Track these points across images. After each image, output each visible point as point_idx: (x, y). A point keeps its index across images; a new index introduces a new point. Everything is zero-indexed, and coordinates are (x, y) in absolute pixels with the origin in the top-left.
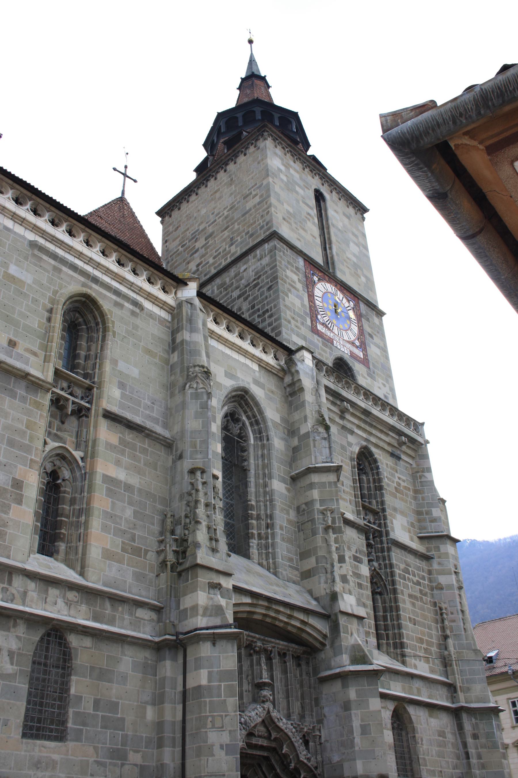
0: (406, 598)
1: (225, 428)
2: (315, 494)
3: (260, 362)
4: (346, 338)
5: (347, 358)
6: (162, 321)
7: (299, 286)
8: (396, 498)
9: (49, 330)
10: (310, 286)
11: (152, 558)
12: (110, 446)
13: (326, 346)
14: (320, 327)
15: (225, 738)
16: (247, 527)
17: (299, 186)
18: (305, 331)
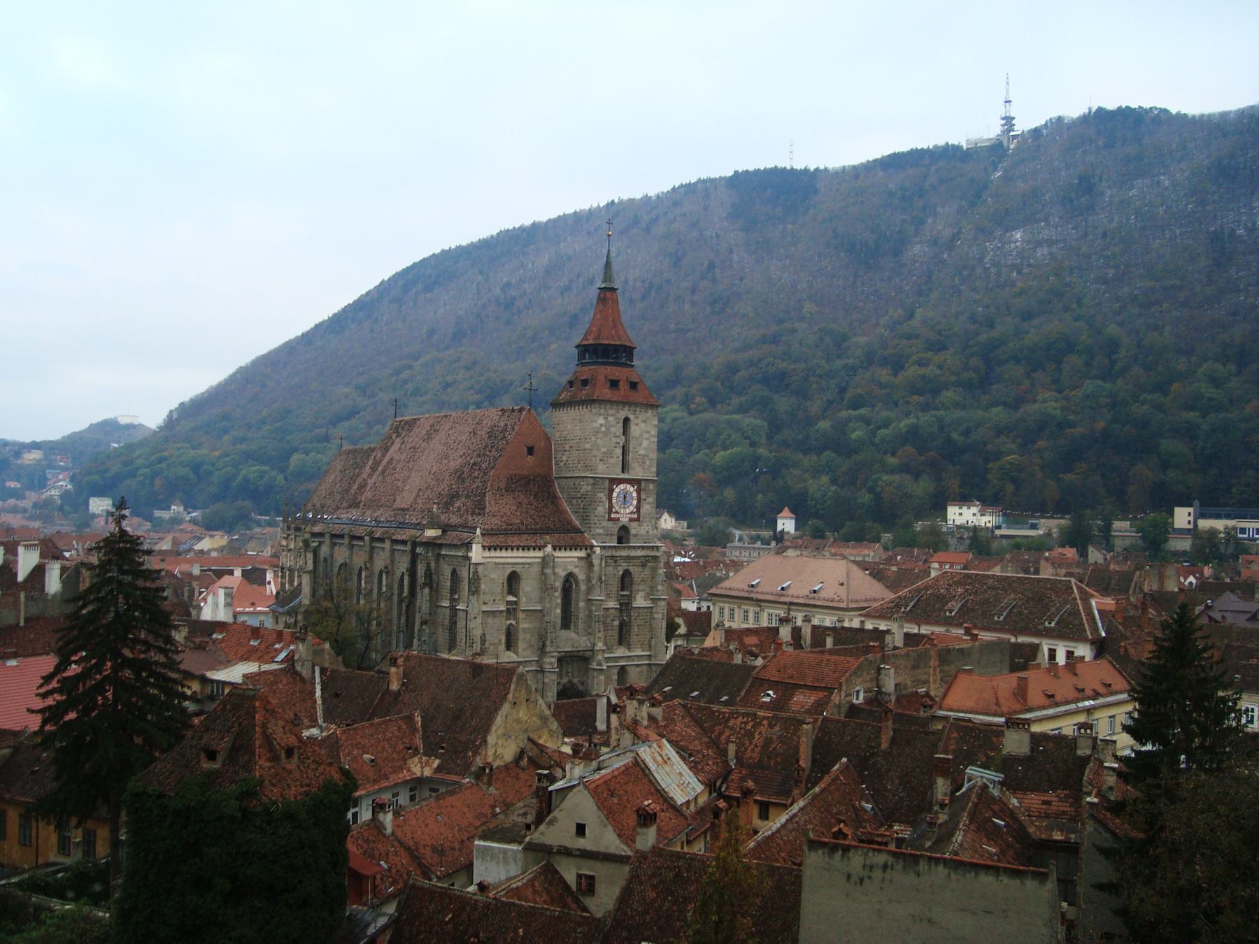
0: (636, 628)
1: (564, 586)
2: (594, 608)
3: (578, 558)
4: (628, 512)
5: (625, 523)
6: (539, 563)
7: (604, 499)
8: (640, 584)
9: (503, 590)
10: (611, 491)
11: (536, 647)
12: (523, 619)
13: (614, 524)
14: (613, 516)
15: (551, 694)
16: (570, 619)
17: (613, 426)
18: (605, 523)
